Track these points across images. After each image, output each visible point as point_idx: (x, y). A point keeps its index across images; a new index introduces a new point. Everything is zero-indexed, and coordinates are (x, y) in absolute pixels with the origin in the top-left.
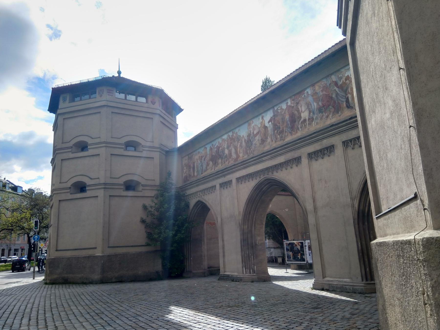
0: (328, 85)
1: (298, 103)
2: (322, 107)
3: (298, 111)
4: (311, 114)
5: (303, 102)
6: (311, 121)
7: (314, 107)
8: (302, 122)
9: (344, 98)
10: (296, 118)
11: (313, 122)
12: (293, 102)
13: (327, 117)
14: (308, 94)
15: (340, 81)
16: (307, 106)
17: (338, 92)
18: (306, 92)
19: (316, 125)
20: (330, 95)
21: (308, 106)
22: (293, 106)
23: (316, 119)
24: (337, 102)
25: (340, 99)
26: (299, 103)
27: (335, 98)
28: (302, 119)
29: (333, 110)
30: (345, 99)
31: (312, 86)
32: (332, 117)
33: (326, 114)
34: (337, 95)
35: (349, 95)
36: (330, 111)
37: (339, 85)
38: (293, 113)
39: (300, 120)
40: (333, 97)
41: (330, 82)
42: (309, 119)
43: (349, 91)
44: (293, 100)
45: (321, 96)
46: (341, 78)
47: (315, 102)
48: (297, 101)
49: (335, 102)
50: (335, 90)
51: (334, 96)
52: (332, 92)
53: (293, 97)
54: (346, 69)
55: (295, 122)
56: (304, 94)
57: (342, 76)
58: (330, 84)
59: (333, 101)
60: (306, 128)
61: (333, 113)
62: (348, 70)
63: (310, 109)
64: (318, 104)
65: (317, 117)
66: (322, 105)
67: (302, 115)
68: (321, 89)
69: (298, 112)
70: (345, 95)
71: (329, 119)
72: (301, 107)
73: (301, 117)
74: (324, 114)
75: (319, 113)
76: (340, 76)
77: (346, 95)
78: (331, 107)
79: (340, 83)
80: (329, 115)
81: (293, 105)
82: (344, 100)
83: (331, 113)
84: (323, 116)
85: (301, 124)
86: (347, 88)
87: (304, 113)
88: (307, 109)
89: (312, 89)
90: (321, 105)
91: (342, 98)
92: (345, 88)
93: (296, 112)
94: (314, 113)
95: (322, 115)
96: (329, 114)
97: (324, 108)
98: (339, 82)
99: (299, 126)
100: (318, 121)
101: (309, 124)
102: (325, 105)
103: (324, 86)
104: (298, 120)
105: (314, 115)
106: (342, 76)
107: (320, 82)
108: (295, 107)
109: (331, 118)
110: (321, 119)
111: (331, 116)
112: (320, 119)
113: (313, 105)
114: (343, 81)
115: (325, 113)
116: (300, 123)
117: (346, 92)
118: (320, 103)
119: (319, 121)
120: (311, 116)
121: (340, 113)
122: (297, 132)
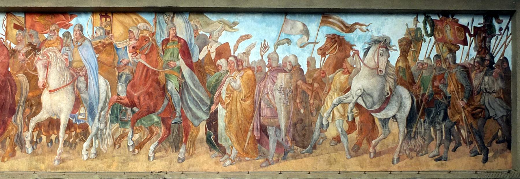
0: (159, 39)
1: (35, 49)
2: (126, 105)
3: (33, 78)
4: (82, 110)
5: (59, 54)
6: (77, 135)
7: (99, 92)
8: (39, 125)
9: (205, 109)
10: (17, 98)
11: (86, 144)
12: (15, 32)
13: (139, 146)
14: (82, 37)
15: (200, 51)
16: (72, 76)
17: (189, 81)
18: (74, 21)
19: (92, 156)
20: (161, 77)
21: (74, 79)
22: (14, 52)
23: (96, 135)
24: (178, 110)
25: (191, 106)
26: (39, 50)
27: (176, 97)
28: (43, 116)
29: (161, 130)
30: (206, 113)
31: (101, 16)
32: (154, 152)
33: (137, 136)
34: (183, 87)
35: (220, 107)
36: (151, 132)
37: (195, 60)
38: (7, 74)
39: (35, 114)
40: (169, 88)
41: (166, 32)
42: (70, 126)
43: (224, 96)
44: (16, 27)
45: (128, 63)
46: (204, 42)
47: (105, 78)
48: (34, 41)
49: (171, 108)
50: (180, 68)
51: (174, 87)
52: (168, 70)
53: (21, 17)
54: (225, 23)
55: (13, 112)
56: (67, 27)
57: (208, 35)
58: (166, 42)
59: (166, 102)
60: (53, 151)
61: (160, 142)
62: (231, 27)
63: (79, 90)
64: (113, 88)
65: (102, 130)
66: (127, 96)
67: (45, 98)
68: (133, 42)
69: (29, 82)
70: (209, 103)
71: (142, 157)
72: (47, 67)
73: (39, 104)
74: (130, 134)
75: (112, 122)
76: (201, 32)
77: (212, 103)
78: (155, 118)
79: (199, 56)
80: (144, 143)
81: (13, 46)
82: (205, 117)
83: (154, 138)
84: (123, 136)
85: (33, 131)
86: (218, 84)
87: (57, 97)
88: (70, 88)
89: (98, 26)
90: (123, 95)
91: (197, 106)
92: (211, 80)
93: (21, 78)
94: (91, 112)
95: (120, 131)
96: (149, 139)
97: (133, 112)
98: (196, 50)
99: (27, 136)
100: (104, 148)
101: (65, 142)
102: (136, 100)
103: (145, 38)
104: (24, 111)
105: (93, 119)
106: (208, 35)
107: (134, 17)
108: (21, 57)
109: (151, 154)
110: (117, 143)
111: (152, 148)
112: (110, 141)
113: (92, 82)
114: (209, 54)
115: (133, 127)
116: (32, 124)
117: (214, 95)
118: (121, 89)
119: (105, 146)
120: (80, 117)
121: (182, 150)
122: (13, 154)
